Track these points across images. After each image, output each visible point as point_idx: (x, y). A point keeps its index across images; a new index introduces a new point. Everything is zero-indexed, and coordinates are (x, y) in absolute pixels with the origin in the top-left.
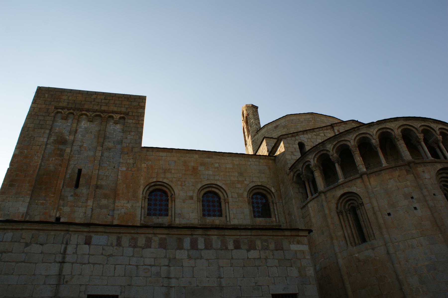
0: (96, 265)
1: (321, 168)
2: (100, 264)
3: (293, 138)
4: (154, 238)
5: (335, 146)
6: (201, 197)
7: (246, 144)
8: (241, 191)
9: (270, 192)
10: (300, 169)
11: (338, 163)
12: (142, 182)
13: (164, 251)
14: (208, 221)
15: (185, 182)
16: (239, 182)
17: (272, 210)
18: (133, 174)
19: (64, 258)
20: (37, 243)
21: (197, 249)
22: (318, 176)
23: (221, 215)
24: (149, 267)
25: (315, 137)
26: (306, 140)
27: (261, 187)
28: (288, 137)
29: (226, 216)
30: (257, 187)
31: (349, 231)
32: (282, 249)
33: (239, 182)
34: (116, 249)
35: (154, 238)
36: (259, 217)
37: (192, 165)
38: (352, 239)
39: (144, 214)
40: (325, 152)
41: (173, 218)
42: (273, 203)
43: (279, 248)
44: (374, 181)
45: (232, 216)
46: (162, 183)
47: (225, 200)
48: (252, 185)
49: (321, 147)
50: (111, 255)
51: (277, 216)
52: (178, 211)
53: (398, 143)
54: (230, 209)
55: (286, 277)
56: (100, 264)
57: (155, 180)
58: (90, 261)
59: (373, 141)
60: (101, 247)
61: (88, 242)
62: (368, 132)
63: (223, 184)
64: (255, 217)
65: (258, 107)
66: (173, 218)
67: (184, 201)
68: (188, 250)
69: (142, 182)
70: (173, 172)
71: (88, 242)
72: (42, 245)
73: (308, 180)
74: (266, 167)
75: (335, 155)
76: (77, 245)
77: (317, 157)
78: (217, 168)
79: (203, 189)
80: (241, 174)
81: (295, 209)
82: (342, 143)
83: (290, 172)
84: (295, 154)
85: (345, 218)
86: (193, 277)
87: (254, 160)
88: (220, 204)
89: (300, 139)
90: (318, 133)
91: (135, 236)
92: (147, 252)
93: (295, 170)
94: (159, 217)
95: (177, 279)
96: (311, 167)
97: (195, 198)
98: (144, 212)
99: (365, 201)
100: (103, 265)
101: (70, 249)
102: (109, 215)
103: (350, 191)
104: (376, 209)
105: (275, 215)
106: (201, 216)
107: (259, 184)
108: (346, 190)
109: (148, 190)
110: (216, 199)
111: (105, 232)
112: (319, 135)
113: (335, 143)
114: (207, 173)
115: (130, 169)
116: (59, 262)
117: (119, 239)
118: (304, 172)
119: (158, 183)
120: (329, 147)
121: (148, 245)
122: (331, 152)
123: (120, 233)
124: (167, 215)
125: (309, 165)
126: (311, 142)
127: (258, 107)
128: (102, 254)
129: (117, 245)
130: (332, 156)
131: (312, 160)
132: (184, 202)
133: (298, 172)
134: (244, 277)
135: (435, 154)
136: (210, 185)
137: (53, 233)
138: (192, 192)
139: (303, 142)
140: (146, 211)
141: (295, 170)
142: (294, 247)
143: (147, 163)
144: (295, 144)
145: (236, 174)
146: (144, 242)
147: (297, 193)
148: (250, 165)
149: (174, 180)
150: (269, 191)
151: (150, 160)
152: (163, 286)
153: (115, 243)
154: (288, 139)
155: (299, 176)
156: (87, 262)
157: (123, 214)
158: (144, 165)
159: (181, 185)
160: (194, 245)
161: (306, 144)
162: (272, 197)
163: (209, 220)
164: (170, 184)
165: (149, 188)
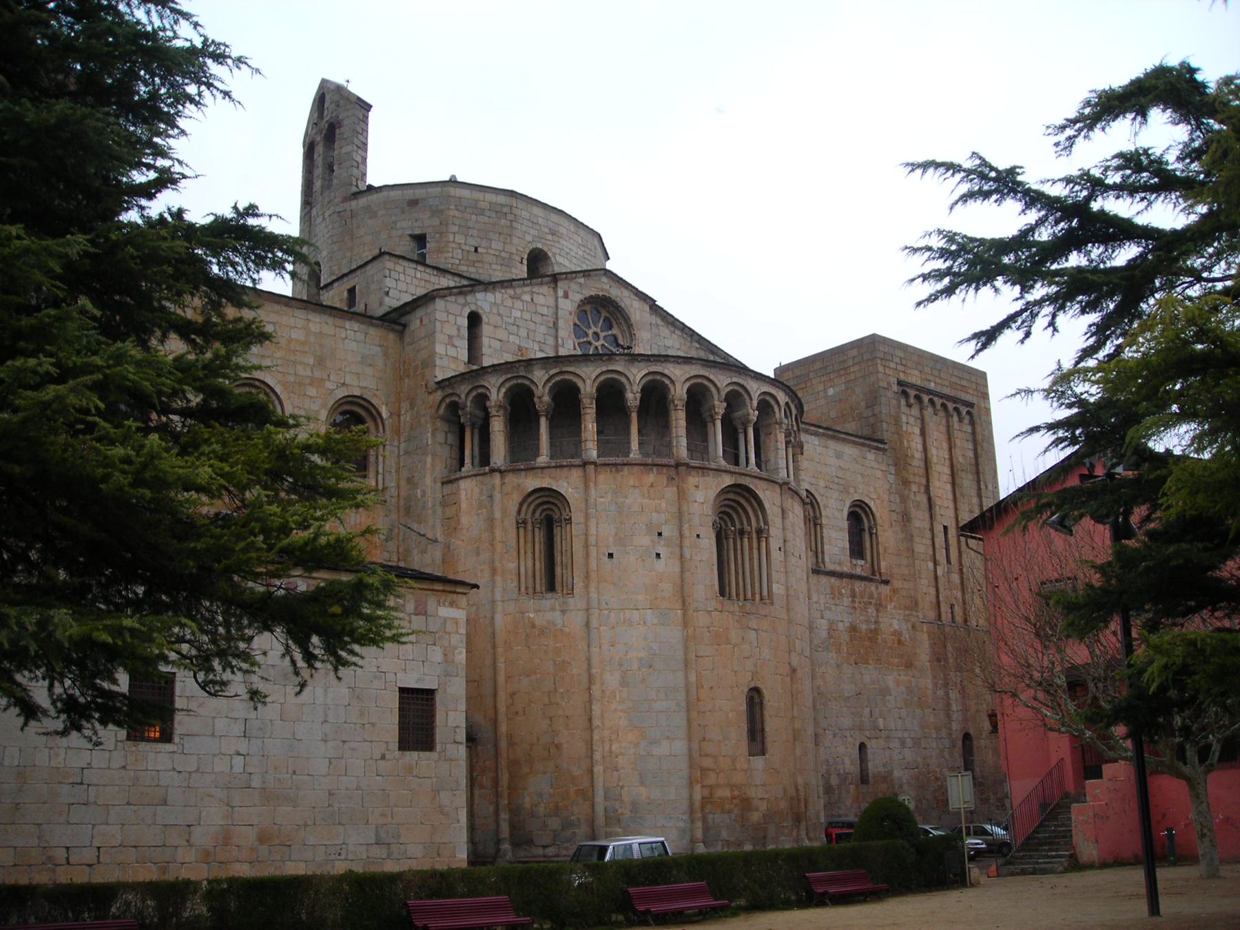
1: (509, 408)
3: (461, 300)
10: (463, 396)
11: (546, 416)
16: (314, 382)
22: (498, 426)
25: (509, 302)
26: (487, 309)
28: (451, 294)
33: (314, 382)
44: (605, 480)
49: (522, 368)
53: (673, 413)
59: (629, 395)
62: (626, 372)
77: (507, 385)
80: (320, 362)
83: (436, 390)
84: (457, 342)
87: (356, 326)
90: (519, 291)
99: (577, 517)
103: (555, 488)
104: (592, 540)
105: (377, 473)
108: (545, 482)
112: (519, 298)
118: (469, 404)
120: (539, 376)
122: (540, 387)
130: (540, 398)
131: (496, 391)
135: (733, 454)
144: (460, 315)
145: (311, 361)
148: (344, 339)
155: (454, 407)
161: (485, 318)
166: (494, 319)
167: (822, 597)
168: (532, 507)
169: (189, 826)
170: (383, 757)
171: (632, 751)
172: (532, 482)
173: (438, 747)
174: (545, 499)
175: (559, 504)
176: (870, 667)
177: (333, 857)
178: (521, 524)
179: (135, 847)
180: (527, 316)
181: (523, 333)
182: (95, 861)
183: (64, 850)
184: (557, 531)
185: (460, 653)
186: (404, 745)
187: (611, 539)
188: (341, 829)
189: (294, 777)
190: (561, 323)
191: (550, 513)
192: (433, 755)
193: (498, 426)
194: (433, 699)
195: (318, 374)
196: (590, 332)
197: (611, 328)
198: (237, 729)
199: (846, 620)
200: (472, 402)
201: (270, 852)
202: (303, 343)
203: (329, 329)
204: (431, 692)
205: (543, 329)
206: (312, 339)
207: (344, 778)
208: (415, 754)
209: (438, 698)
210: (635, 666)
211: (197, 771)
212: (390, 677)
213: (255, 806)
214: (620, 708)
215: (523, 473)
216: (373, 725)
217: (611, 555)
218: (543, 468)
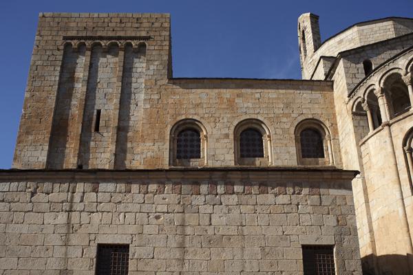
1: (390, 93)
8: (287, 127)
15: (218, 118)
19: (71, 207)
22: (382, 103)
33: (285, 115)
36: (309, 157)
55: (320, 226)
57: (183, 117)
61: (95, 190)
65: (318, 17)
71: (95, 190)
77: (384, 78)
79: (242, 126)
80: (287, 105)
93: (355, 98)
96: (375, 92)
97: (232, 137)
98: (173, 155)
101: (77, 198)
106: (239, 156)
107: (310, 117)
109: (176, 129)
118: (366, 99)
119: (188, 121)
123: (129, 179)
127: (318, 17)
133: (359, 100)
141: (355, 98)
145: (282, 106)
159: (214, 122)
165: (178, 127)
193: (382, 103)
195: (286, 111)
200: (368, 97)
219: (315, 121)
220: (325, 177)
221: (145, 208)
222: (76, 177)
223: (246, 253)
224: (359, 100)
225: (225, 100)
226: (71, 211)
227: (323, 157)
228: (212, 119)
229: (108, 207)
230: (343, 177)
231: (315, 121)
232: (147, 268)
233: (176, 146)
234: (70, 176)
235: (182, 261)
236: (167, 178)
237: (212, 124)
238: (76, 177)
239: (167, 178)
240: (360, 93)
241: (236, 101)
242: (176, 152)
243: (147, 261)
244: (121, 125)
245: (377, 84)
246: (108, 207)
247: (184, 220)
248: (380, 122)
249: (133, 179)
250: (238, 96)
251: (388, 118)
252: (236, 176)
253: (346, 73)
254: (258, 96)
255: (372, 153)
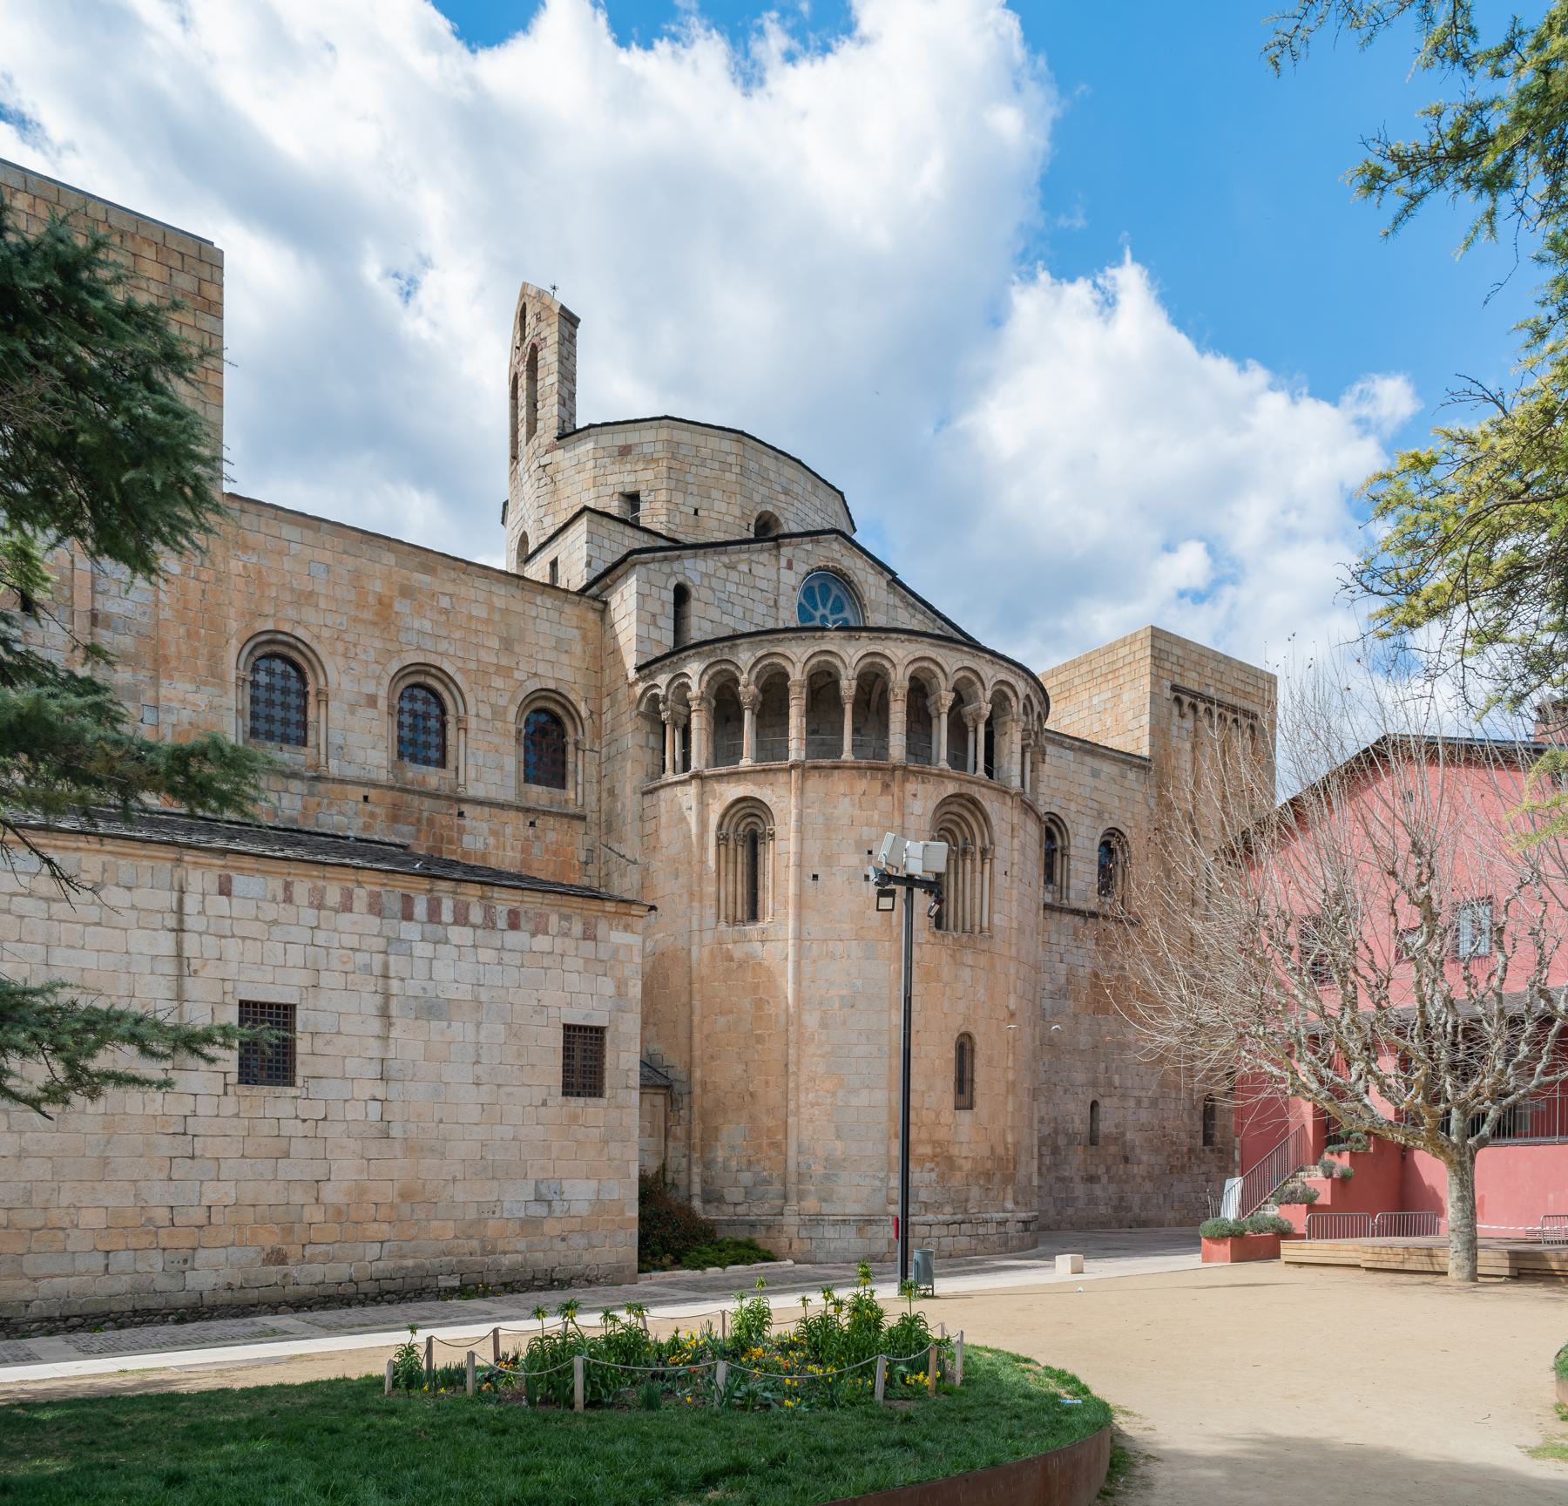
0: (248, 942)
1: (714, 703)
2: (255, 939)
4: (357, 890)
5: (759, 661)
6: (395, 702)
7: (514, 457)
9: (574, 714)
10: (664, 687)
11: (753, 710)
12: (234, 626)
13: (378, 920)
14: (410, 775)
15: (355, 645)
17: (570, 767)
18: (203, 591)
19: (181, 921)
20: (117, 885)
21: (440, 923)
23: (442, 763)
24: (350, 952)
27: (554, 695)
29: (457, 768)
30: (544, 693)
31: (731, 888)
32: (595, 939)
34: (284, 909)
35: (357, 890)
36: (538, 782)
37: (377, 590)
38: (731, 905)
39: (244, 732)
40: (732, 668)
41: (323, 757)
42: (577, 749)
43: (589, 935)
45: (472, 774)
46: (291, 640)
47: (459, 720)
48: (532, 685)
50: (275, 922)
51: (580, 788)
52: (336, 739)
54: (469, 751)
56: (255, 939)
57: (270, 626)
58: (236, 933)
60: (254, 902)
61: (225, 890)
63: (459, 669)
64: (526, 780)
65: (578, 320)
66: (323, 757)
67: (352, 708)
68: (422, 923)
69: (236, 628)
70: (323, 604)
71: (225, 890)
72: (129, 889)
73: (675, 725)
74: (576, 632)
75: (752, 688)
76: (203, 894)
78: (446, 612)
80: (507, 644)
81: (628, 789)
82: (776, 660)
85: (731, 852)
86: (431, 979)
87: (549, 602)
88: (444, 725)
89: (684, 574)
91: (321, 883)
92: (345, 918)
94: (285, 747)
95: (402, 980)
96: (689, 695)
98: (244, 725)
100: (262, 941)
101: (191, 904)
102: (142, 721)
106: (395, 758)
107: (552, 686)
109: (251, 653)
110: (435, 711)
111: (258, 870)
113: (760, 653)
114: (416, 624)
115: (193, 574)
116: (173, 930)
117: (288, 886)
118: (670, 697)
119: (280, 637)
121: (347, 907)
123: (289, 874)
124: (303, 742)
125: (687, 687)
126: (712, 589)
127: (578, 320)
128: (257, 919)
129: (284, 901)
132: (352, 713)
133: (656, 691)
134: (519, 987)
136: (423, 668)
137: (146, 863)
138: (374, 682)
139: (689, 584)
140: (248, 722)
142: (618, 937)
143: (245, 558)
145: (495, 643)
146: (338, 899)
147: (641, 747)
149: (326, 633)
150: (571, 709)
151: (254, 549)
152: (376, 992)
153: (280, 896)
154: (652, 566)
156: (229, 934)
157: (186, 726)
158: (235, 566)
160: (434, 914)
162: (576, 730)
163: (413, 772)
164: (314, 645)
165: (255, 648)
166: (705, 594)
167: (1063, 938)
168: (735, 820)
169: (317, 1181)
170: (544, 1104)
171: (829, 1100)
172: (734, 791)
173: (608, 1093)
174: (748, 811)
175: (763, 816)
176: (1110, 1018)
177: (486, 1215)
178: (722, 840)
179: (254, 1206)
180: (744, 591)
181: (738, 612)
182: (205, 1222)
183: (168, 1210)
184: (760, 848)
185: (634, 986)
186: (569, 1090)
187: (816, 859)
188: (496, 1183)
189: (441, 1125)
190: (782, 601)
191: (753, 826)
192: (602, 1102)
194: (602, 1039)
196: (818, 614)
197: (841, 609)
198: (373, 1070)
199: (1087, 964)
201: (413, 1210)
202: (487, 621)
203: (517, 606)
204: (600, 1031)
205: (762, 609)
206: (497, 617)
207: (498, 1127)
208: (581, 1101)
209: (608, 1036)
210: (837, 1006)
211: (325, 1119)
212: (553, 1012)
213: (395, 1158)
214: (819, 1052)
215: (726, 779)
216: (532, 1066)
217: (815, 877)
218: (745, 773)
219: (558, 697)
220: (607, 909)
221: (321, 937)
222: (186, 858)
223: (483, 1033)
224: (656, 691)
225: (372, 600)
226: (182, 930)
227: (564, 787)
228: (340, 646)
229: (253, 929)
230: (633, 912)
231: (558, 697)
232: (329, 1050)
233: (247, 701)
234: (173, 856)
235: (384, 1038)
236: (357, 881)
237: (340, 660)
238: (186, 858)
239: (357, 881)
240: (662, 680)
241: (397, 607)
242: (248, 717)
243: (328, 1037)
244: (98, 606)
245: (696, 679)
246: (253, 929)
247: (386, 966)
248: (686, 767)
249: (296, 875)
250: (406, 592)
251: (703, 762)
252: (472, 892)
253: (640, 608)
254: (445, 602)
255: (663, 820)
